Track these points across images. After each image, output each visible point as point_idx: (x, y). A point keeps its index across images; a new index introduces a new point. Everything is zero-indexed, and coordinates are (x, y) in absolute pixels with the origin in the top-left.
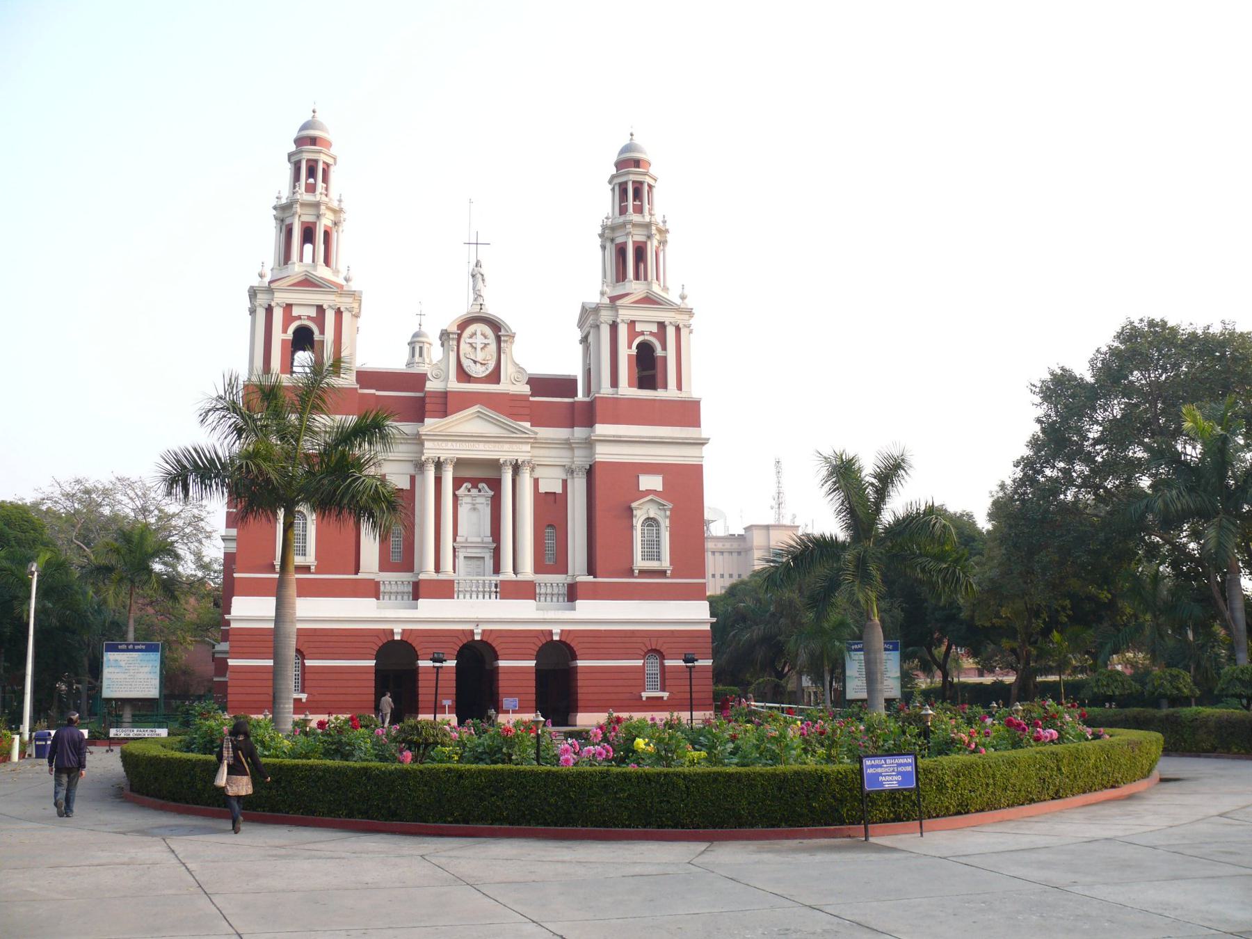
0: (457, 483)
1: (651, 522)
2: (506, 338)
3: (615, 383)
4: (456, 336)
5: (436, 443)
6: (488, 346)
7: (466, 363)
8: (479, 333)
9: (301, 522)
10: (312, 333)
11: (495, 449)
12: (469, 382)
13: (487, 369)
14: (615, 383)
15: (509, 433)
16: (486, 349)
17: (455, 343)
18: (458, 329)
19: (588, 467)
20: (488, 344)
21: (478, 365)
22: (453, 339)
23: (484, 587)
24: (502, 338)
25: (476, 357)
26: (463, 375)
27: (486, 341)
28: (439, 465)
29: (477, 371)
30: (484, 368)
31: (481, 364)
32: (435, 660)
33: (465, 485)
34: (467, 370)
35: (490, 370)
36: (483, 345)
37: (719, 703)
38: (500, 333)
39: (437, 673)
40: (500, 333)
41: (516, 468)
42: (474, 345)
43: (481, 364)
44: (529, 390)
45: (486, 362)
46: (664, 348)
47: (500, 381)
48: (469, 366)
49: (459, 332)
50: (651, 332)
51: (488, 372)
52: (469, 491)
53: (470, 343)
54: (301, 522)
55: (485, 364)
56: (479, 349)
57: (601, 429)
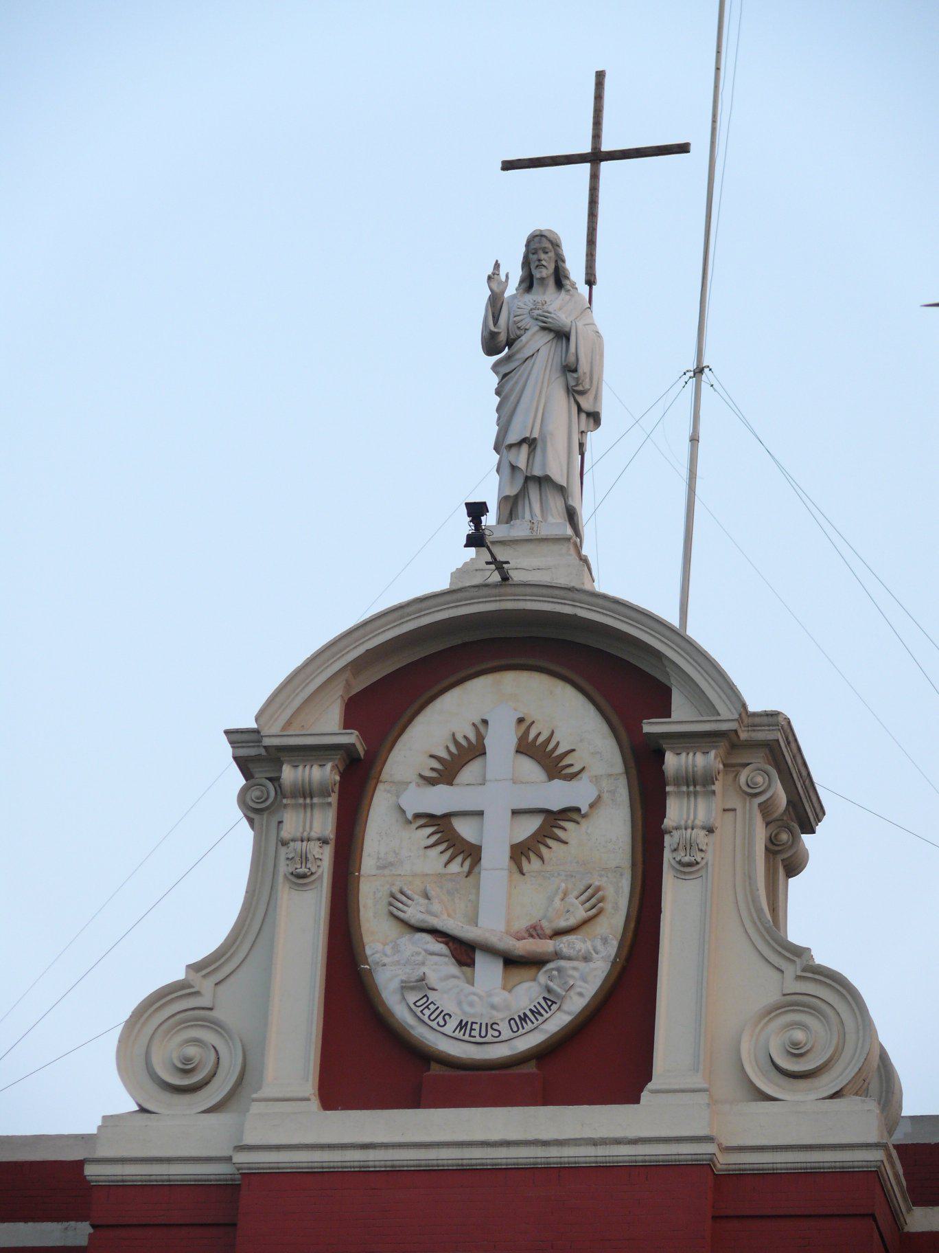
2: (701, 761)
4: (323, 773)
6: (571, 831)
8: (501, 741)
12: (414, 1099)
13: (551, 1000)
16: (554, 852)
17: (324, 822)
18: (349, 722)
20: (570, 813)
21: (488, 971)
22: (305, 793)
24: (672, 762)
25: (474, 921)
27: (557, 795)
30: (527, 993)
31: (512, 962)
34: (400, 1010)
35: (576, 1004)
36: (531, 825)
38: (652, 727)
40: (652, 727)
42: (465, 829)
43: (512, 962)
45: (548, 946)
47: (645, 1074)
48: (421, 984)
49: (351, 738)
51: (556, 1022)
53: (429, 819)
55: (535, 963)
56: (495, 856)
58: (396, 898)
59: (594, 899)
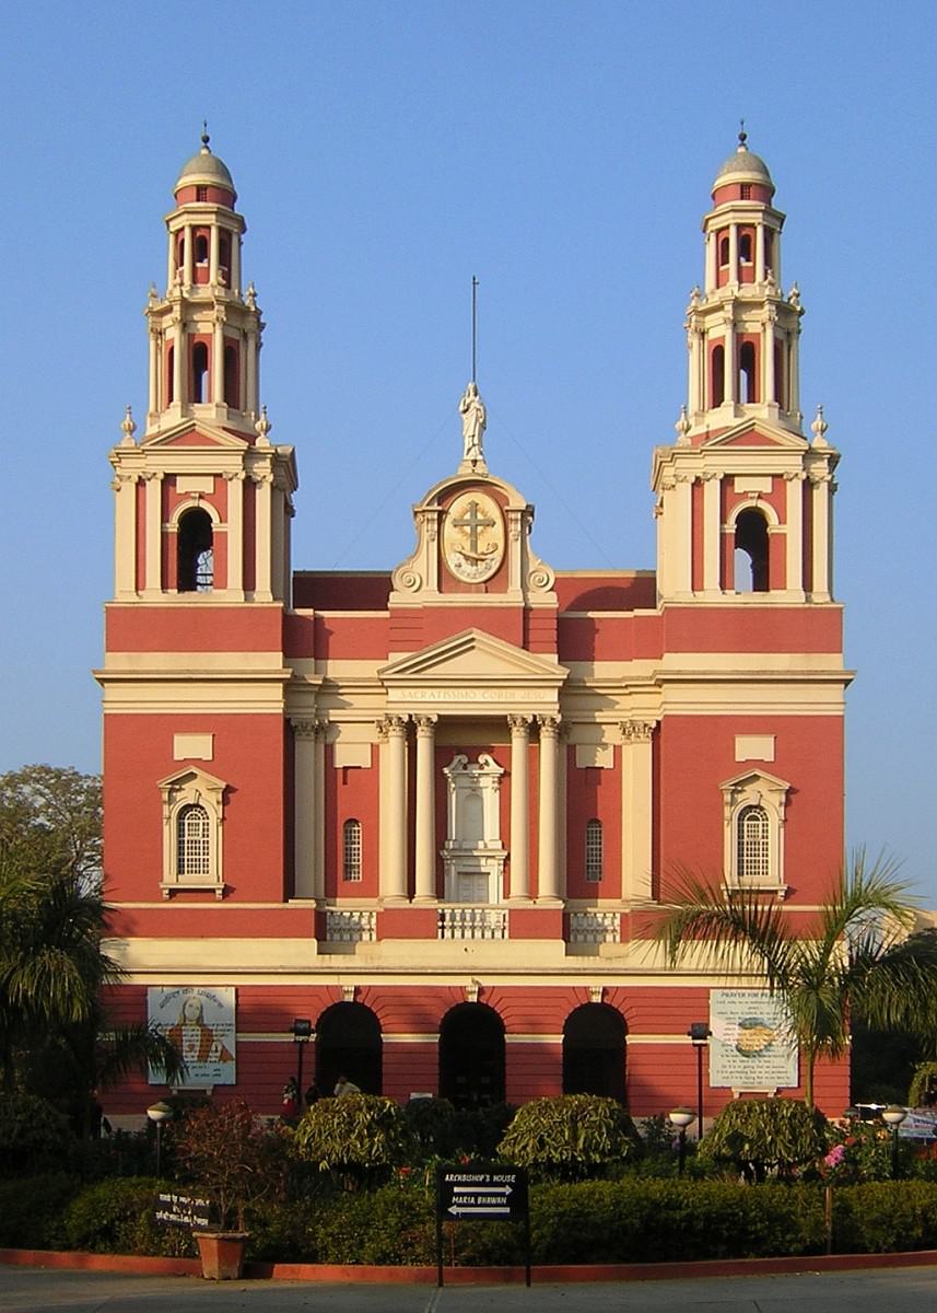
0: (441, 757)
1: (752, 812)
3: (697, 584)
5: (407, 691)
7: (452, 560)
9: (201, 822)
10: (211, 521)
11: (501, 700)
14: (697, 584)
15: (511, 667)
19: (654, 725)
23: (473, 920)
26: (445, 579)
28: (410, 729)
29: (466, 573)
32: (298, 1032)
33: (457, 759)
37: (430, 1095)
39: (301, 1052)
41: (533, 730)
44: (555, 601)
46: (782, 520)
50: (760, 493)
52: (465, 768)
54: (201, 822)
57: (675, 662)
58: (452, 545)
59: (496, 547)
